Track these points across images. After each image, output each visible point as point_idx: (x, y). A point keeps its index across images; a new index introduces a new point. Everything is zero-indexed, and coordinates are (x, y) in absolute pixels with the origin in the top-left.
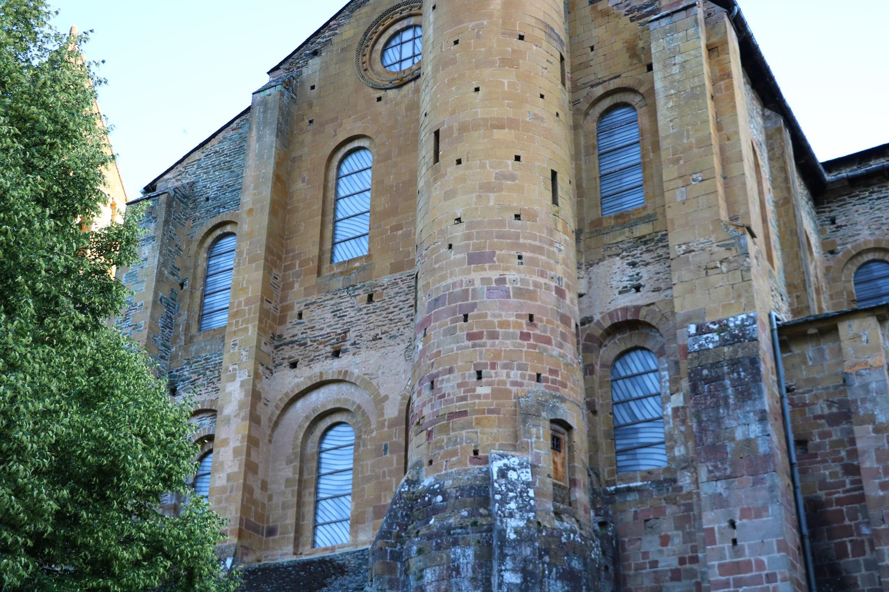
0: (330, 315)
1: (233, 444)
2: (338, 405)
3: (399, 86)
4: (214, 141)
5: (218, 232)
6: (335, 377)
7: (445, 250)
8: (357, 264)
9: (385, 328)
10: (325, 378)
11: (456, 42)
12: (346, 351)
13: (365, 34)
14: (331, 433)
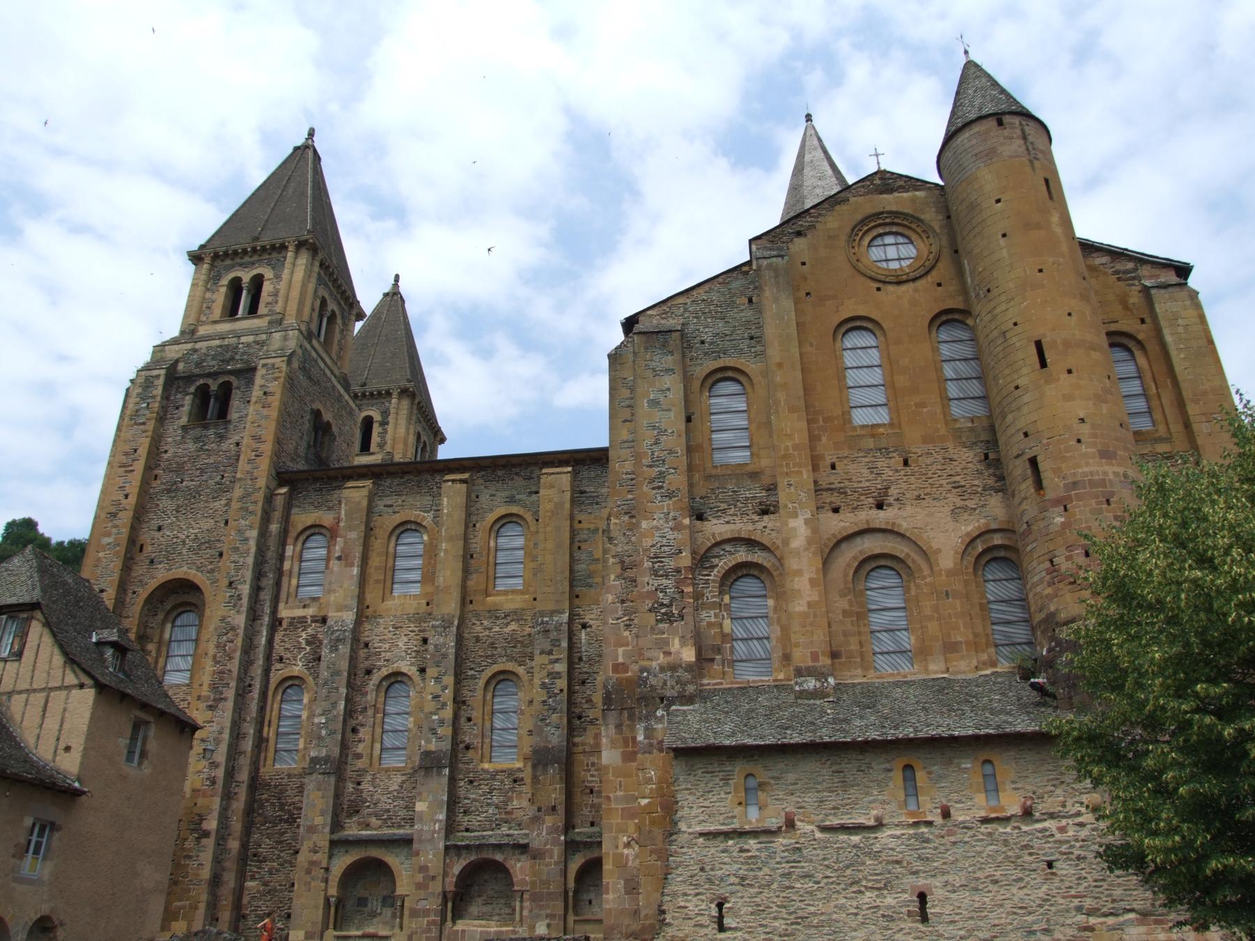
0: (866, 472)
1: (807, 576)
2: (886, 551)
3: (899, 283)
4: (701, 290)
5: (719, 375)
6: (883, 526)
7: (1073, 443)
8: (881, 430)
9: (927, 491)
10: (872, 526)
11: (1040, 271)
12: (890, 505)
13: (853, 230)
14: (873, 574)
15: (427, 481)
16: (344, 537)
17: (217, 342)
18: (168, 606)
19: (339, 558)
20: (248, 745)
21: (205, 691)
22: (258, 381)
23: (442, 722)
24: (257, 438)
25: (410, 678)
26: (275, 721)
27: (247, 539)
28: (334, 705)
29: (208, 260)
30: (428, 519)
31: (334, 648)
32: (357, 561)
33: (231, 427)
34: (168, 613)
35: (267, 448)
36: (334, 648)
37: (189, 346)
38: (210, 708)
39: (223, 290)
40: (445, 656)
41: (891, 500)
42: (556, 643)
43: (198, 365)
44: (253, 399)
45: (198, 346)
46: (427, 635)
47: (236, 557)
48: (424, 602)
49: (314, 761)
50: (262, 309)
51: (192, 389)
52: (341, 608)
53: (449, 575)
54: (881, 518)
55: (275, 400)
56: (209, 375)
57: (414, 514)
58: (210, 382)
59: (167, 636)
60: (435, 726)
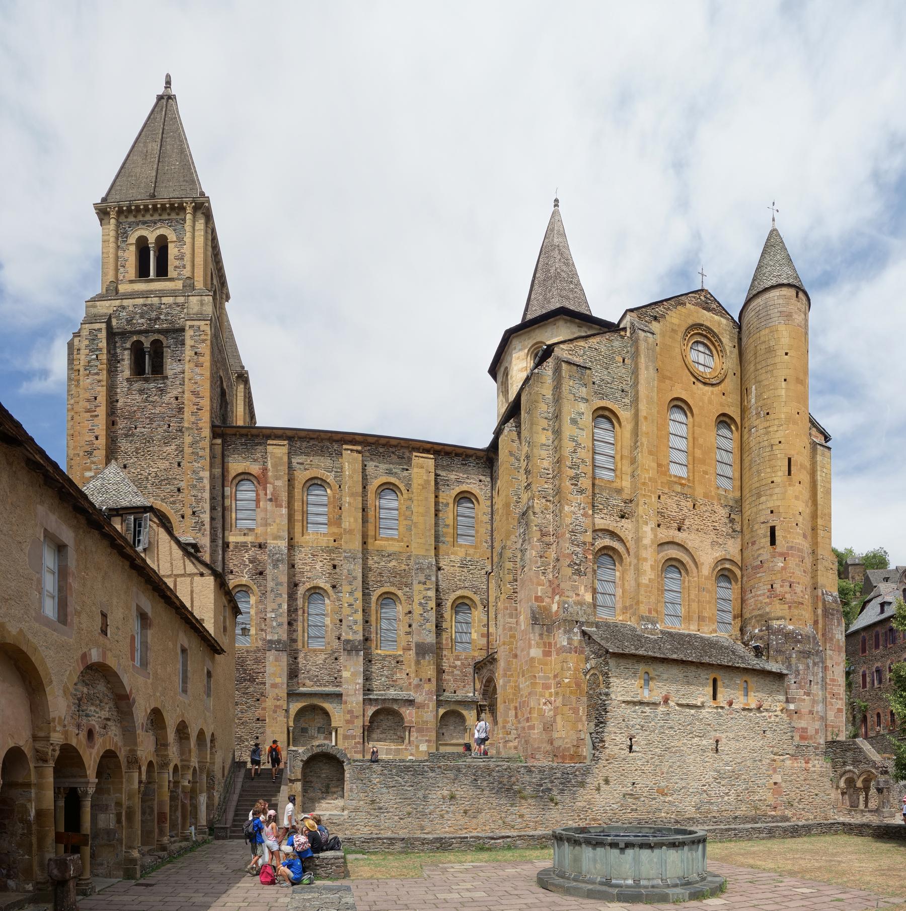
15: (328, 448)
16: (273, 484)
17: (140, 301)
19: (271, 500)
23: (356, 622)
25: (325, 591)
27: (201, 478)
29: (113, 215)
30: (330, 478)
31: (275, 566)
32: (285, 504)
33: (169, 382)
36: (275, 566)
37: (117, 303)
39: (133, 248)
40: (355, 578)
41: (685, 527)
42: (428, 577)
43: (129, 322)
46: (336, 562)
47: (194, 492)
48: (332, 539)
52: (276, 537)
53: (351, 520)
54: (680, 537)
56: (140, 332)
57: (320, 473)
58: (143, 339)
60: (351, 624)
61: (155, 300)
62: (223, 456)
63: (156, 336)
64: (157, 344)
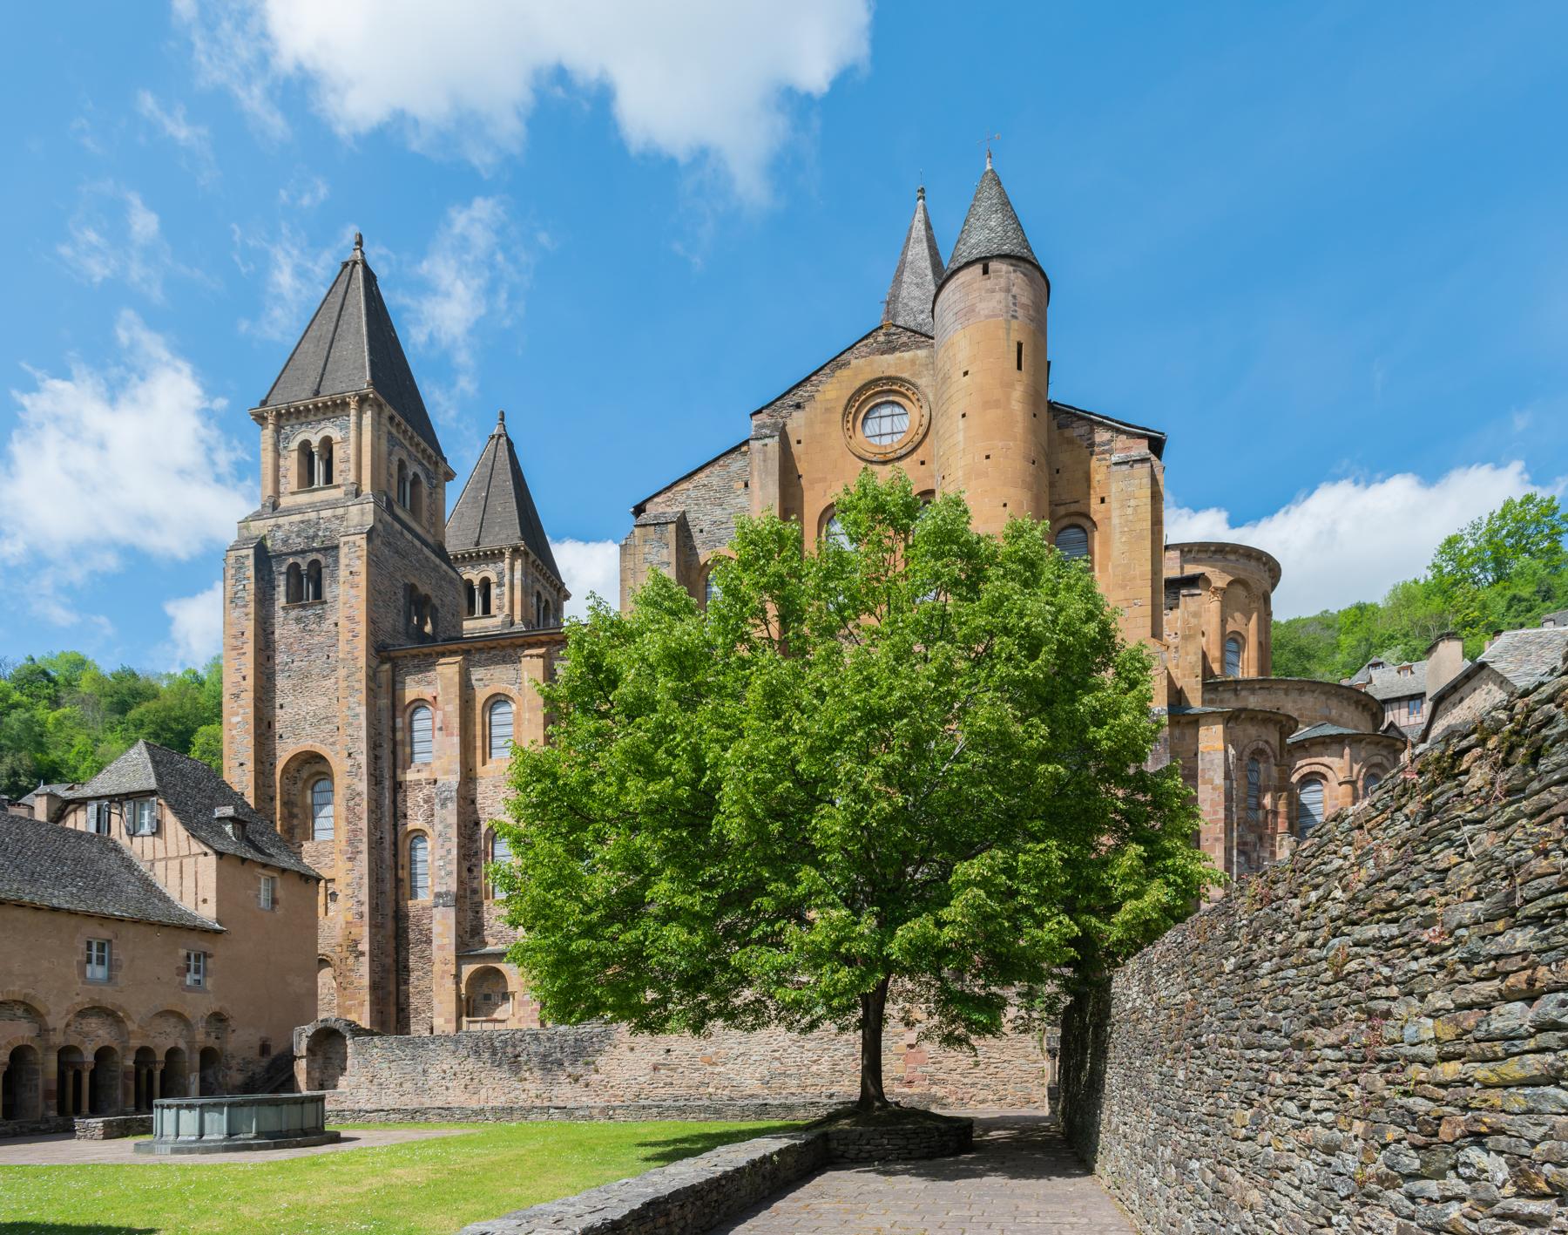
17: (298, 518)
18: (305, 774)
20: (389, 886)
21: (343, 845)
22: (343, 561)
24: (350, 618)
26: (407, 865)
28: (449, 851)
31: (443, 805)
34: (306, 781)
35: (362, 629)
36: (443, 805)
38: (350, 859)
39: (295, 455)
43: (285, 542)
44: (342, 580)
45: (281, 521)
47: (350, 731)
49: (438, 895)
50: (337, 479)
51: (284, 569)
52: (447, 772)
55: (362, 580)
56: (295, 553)
58: (299, 560)
59: (309, 801)
61: (313, 515)
62: (394, 683)
63: (314, 556)
64: (315, 564)
